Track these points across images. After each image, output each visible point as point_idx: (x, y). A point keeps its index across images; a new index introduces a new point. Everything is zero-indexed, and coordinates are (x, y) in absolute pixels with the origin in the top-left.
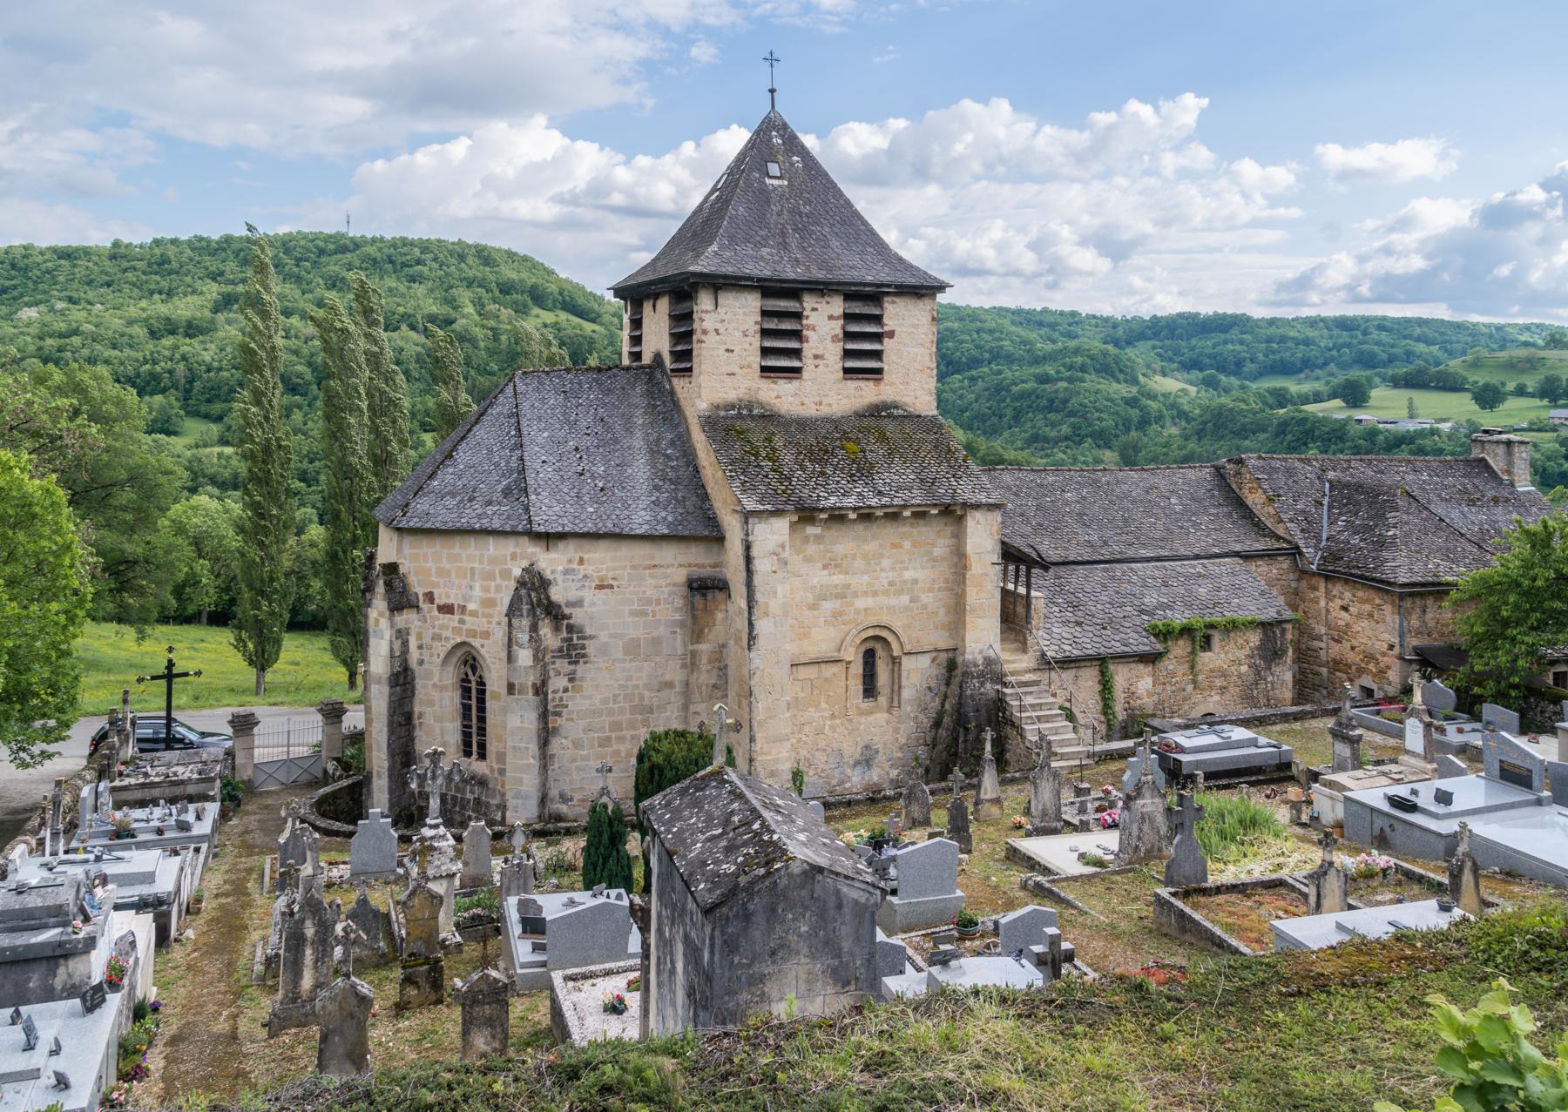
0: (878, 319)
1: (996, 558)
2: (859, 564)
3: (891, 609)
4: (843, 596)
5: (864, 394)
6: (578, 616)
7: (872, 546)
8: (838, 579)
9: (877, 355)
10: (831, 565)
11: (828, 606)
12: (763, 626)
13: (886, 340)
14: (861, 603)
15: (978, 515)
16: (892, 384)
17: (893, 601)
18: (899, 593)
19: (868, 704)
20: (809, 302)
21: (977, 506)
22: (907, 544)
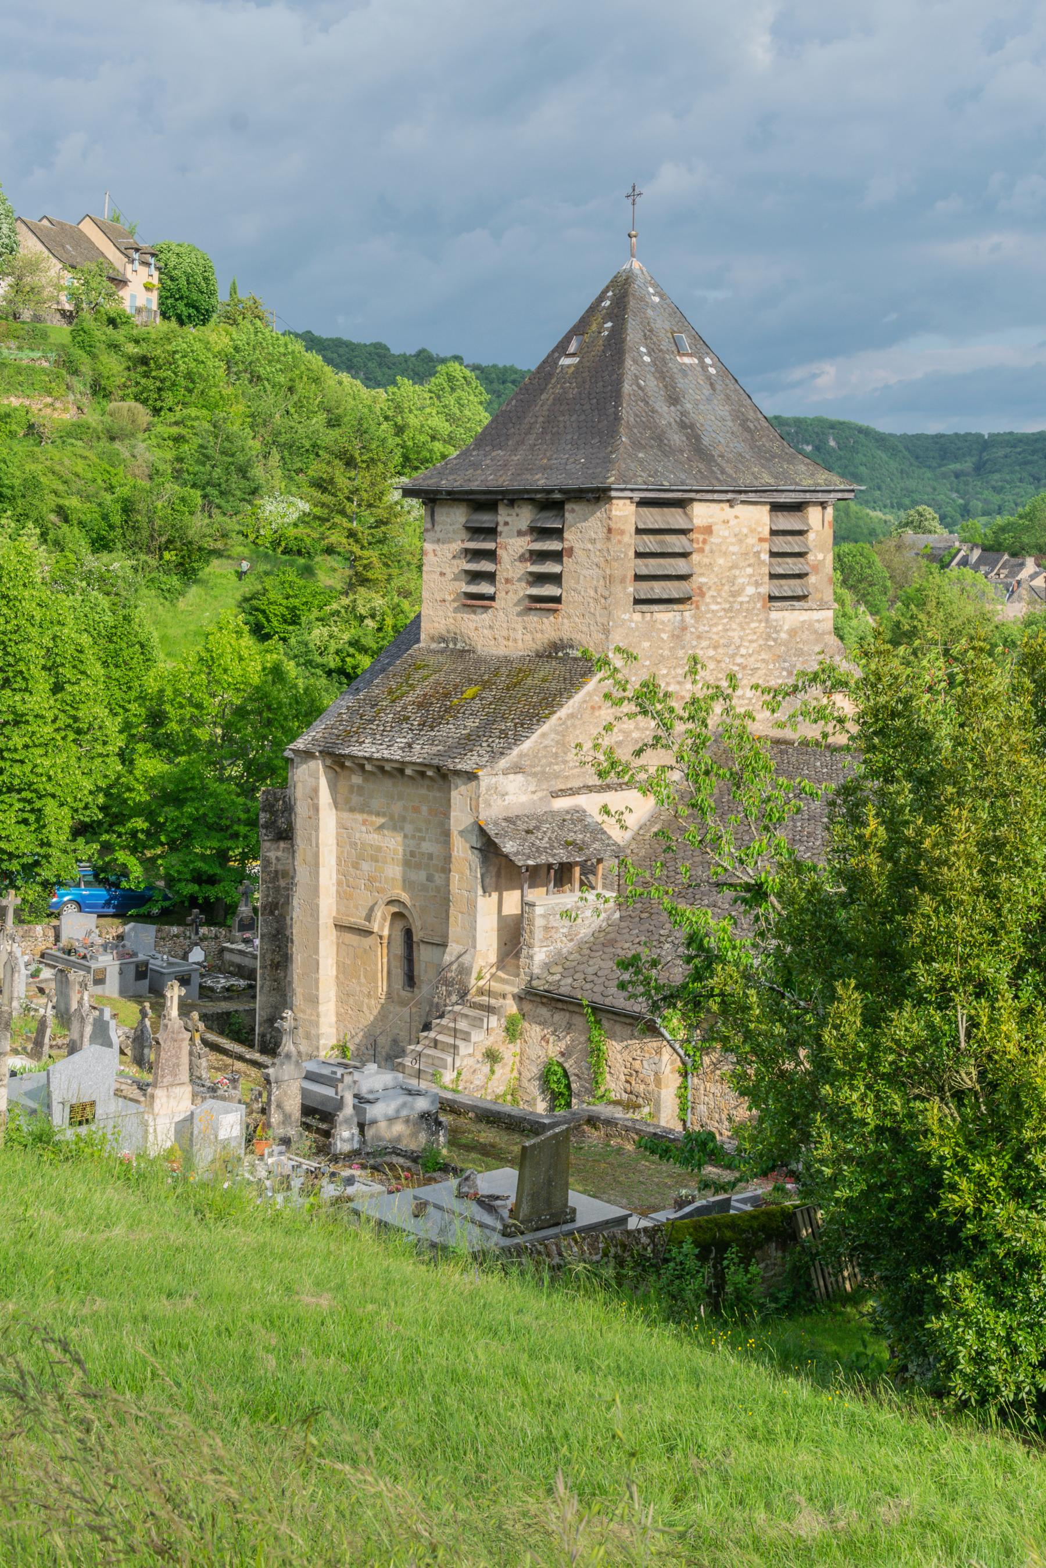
0: (557, 534)
4: (377, 861)
9: (556, 579)
11: (365, 866)
13: (565, 559)
15: (459, 781)
16: (569, 617)
18: (418, 866)
20: (503, 515)
21: (457, 773)
22: (424, 809)
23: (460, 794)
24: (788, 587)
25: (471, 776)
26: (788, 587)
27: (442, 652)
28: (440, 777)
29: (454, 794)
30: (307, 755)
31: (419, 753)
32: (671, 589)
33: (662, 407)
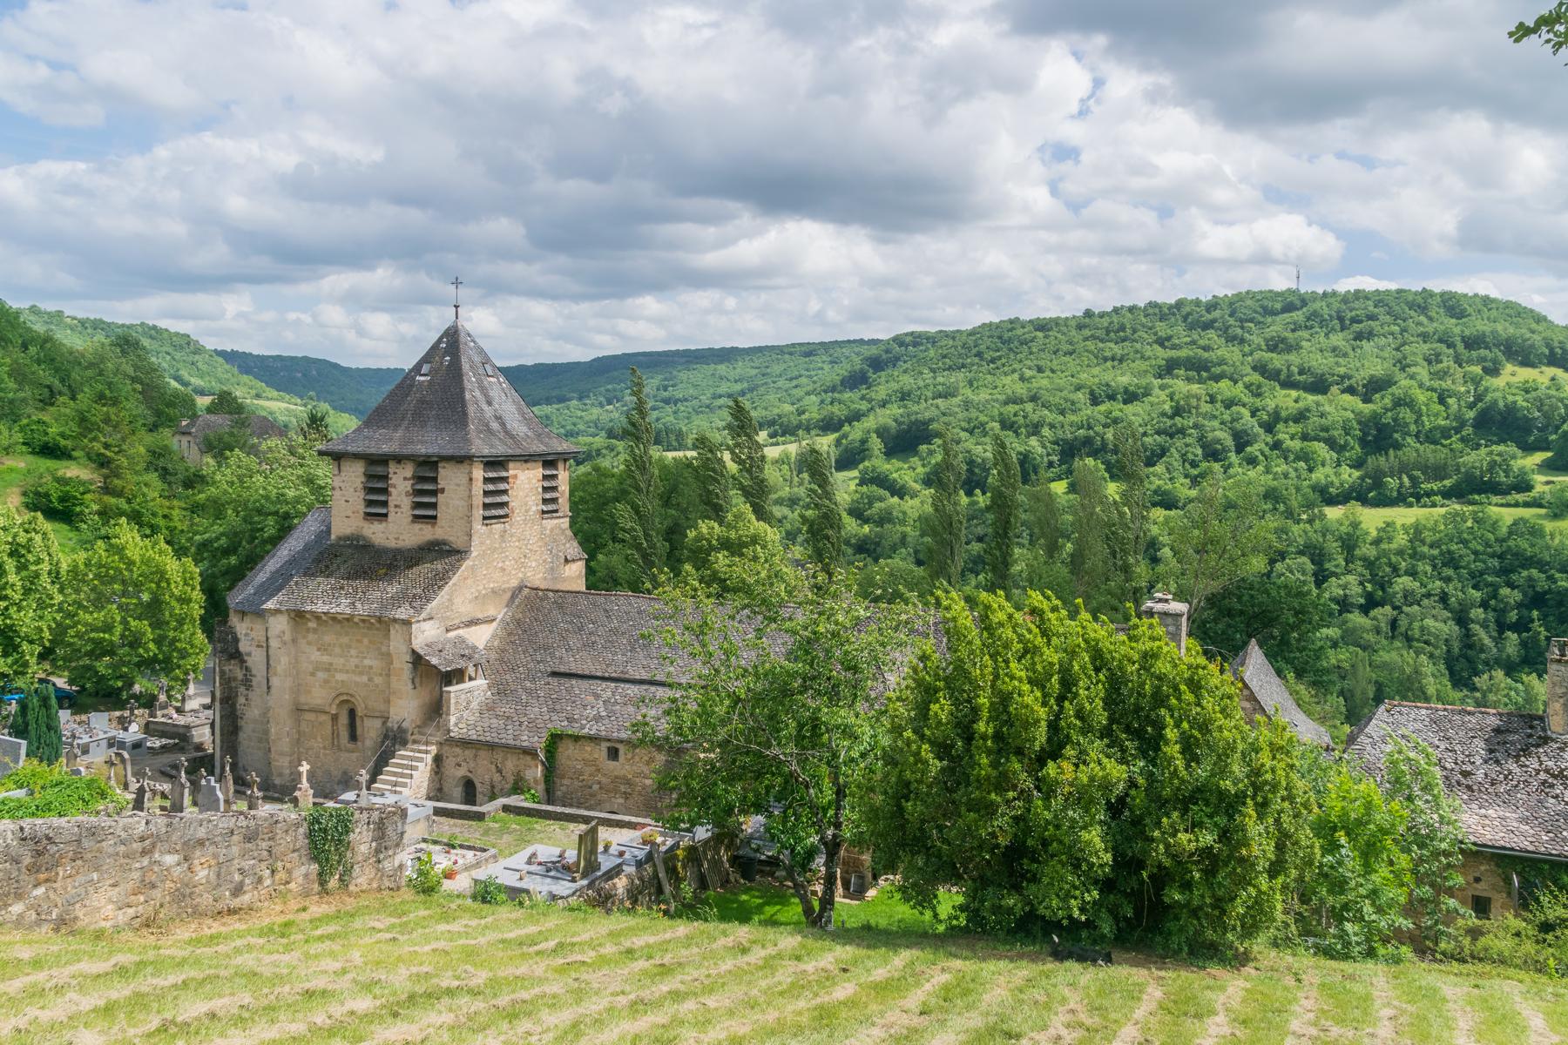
1: (408, 658)
2: (337, 650)
3: (357, 684)
4: (328, 670)
5: (424, 533)
6: (250, 662)
7: (345, 640)
8: (326, 658)
10: (323, 649)
11: (321, 675)
12: (275, 681)
14: (339, 677)
17: (357, 679)
18: (361, 673)
19: (350, 746)
21: (395, 620)
22: (366, 641)
23: (396, 633)
24: (550, 507)
25: (407, 623)
26: (550, 507)
27: (349, 546)
28: (382, 624)
29: (392, 632)
30: (278, 611)
31: (362, 609)
32: (500, 512)
33: (485, 407)
